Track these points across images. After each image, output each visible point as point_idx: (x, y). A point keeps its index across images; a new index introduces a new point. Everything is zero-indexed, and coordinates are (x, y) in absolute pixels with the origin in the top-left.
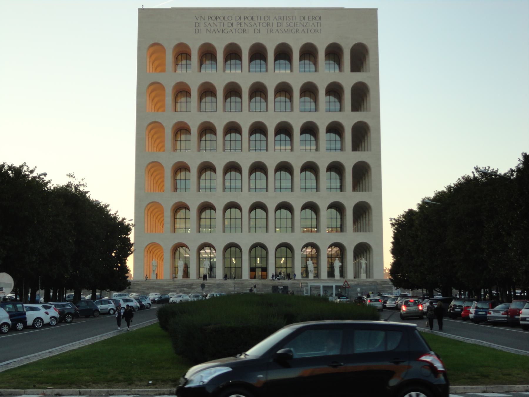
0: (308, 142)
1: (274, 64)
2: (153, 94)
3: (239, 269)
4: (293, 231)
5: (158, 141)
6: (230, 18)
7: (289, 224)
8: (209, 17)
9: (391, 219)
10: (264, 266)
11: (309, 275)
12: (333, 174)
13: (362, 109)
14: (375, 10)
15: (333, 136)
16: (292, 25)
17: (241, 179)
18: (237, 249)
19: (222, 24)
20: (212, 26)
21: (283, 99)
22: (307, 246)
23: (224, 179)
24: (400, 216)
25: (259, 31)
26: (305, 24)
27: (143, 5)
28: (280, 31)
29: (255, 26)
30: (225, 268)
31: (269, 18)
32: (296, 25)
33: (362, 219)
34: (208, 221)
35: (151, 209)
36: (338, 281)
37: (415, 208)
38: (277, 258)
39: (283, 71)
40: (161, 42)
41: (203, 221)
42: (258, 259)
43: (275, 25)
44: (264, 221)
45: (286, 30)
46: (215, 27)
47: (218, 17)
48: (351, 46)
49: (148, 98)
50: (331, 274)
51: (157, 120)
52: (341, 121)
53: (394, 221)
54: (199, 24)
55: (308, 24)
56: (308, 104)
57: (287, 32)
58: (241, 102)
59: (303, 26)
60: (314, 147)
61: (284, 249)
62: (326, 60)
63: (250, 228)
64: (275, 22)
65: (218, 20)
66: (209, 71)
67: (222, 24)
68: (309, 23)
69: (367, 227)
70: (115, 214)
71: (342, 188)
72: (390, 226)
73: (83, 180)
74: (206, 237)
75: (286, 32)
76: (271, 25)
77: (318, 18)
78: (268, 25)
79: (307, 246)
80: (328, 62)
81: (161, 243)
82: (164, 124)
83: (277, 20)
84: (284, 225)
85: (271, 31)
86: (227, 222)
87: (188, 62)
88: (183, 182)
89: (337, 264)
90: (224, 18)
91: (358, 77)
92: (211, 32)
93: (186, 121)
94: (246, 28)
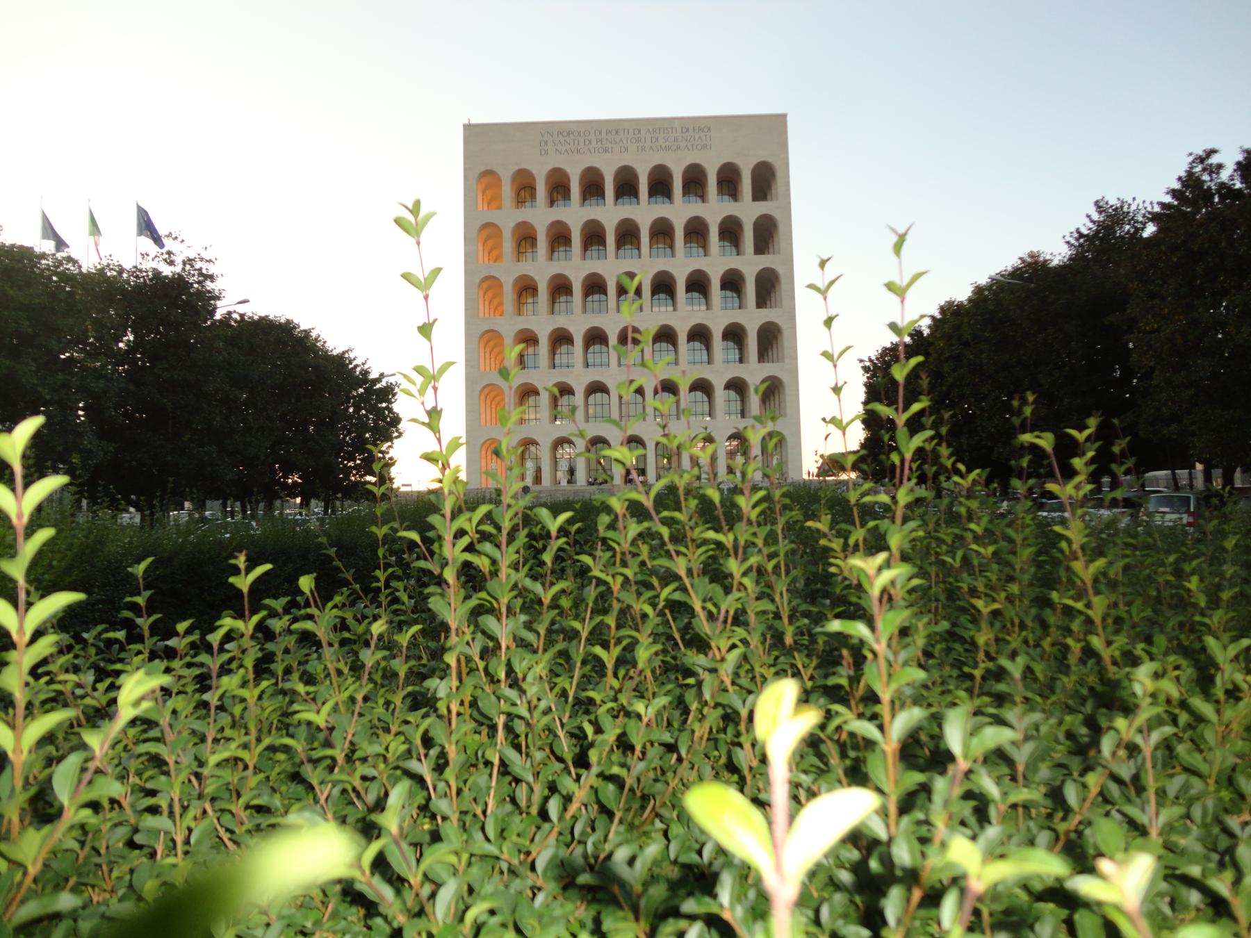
0: (696, 301)
6: (587, 133)
10: (641, 466)
12: (731, 344)
13: (771, 250)
15: (729, 293)
25: (627, 149)
31: (639, 131)
35: (492, 395)
43: (648, 141)
46: (568, 147)
48: (751, 166)
49: (481, 248)
52: (740, 268)
53: (868, 364)
54: (546, 143)
60: (704, 307)
64: (648, 136)
70: (363, 364)
71: (741, 361)
74: (563, 427)
77: (706, 130)
78: (639, 140)
82: (502, 280)
85: (643, 149)
86: (591, 411)
91: (762, 208)
93: (531, 274)
94: (609, 145)
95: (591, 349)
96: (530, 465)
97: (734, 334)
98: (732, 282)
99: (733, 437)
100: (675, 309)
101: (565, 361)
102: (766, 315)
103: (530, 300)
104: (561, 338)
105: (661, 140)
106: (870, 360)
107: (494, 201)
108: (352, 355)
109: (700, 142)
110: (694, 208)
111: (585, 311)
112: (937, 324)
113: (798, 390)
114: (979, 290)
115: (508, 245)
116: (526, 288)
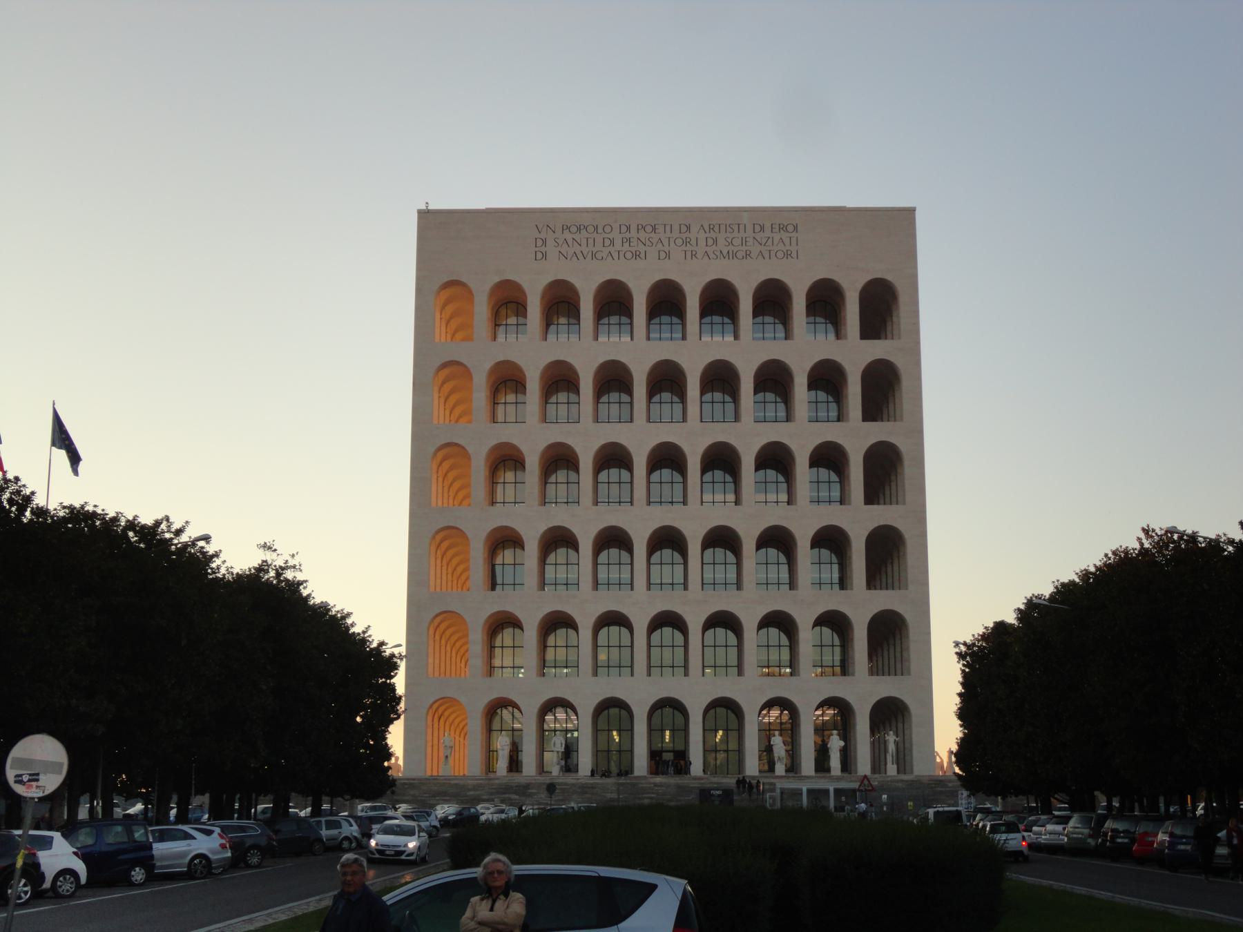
1: (701, 324)
2: (447, 387)
3: (627, 752)
4: (740, 672)
5: (457, 485)
6: (608, 229)
7: (733, 660)
8: (565, 227)
9: (957, 644)
10: (680, 747)
11: (776, 766)
12: (825, 553)
13: (885, 416)
14: (912, 211)
15: (824, 473)
16: (737, 242)
17: (632, 564)
18: (624, 712)
19: (591, 241)
20: (571, 246)
21: (718, 396)
22: (769, 704)
23: (595, 564)
24: (976, 636)
25: (668, 255)
26: (764, 241)
27: (427, 203)
28: (712, 256)
29: (660, 245)
30: (596, 752)
31: (688, 228)
32: (746, 241)
33: (885, 648)
34: (561, 653)
35: (443, 627)
36: (838, 779)
37: (1011, 619)
38: (708, 730)
39: (717, 338)
40: (464, 280)
41: (550, 652)
42: (668, 733)
43: (702, 243)
44: (680, 652)
45: (725, 253)
46: (577, 249)
47: (582, 227)
48: (860, 286)
49: (436, 396)
51: (455, 441)
53: (963, 648)
54: (544, 242)
55: (770, 240)
56: (771, 407)
57: (727, 257)
58: (631, 403)
59: (761, 244)
60: (784, 497)
61: (721, 711)
62: (808, 315)
63: (649, 667)
64: (702, 236)
65: (584, 232)
66: (563, 337)
67: (591, 241)
68: (773, 238)
69: (899, 666)
72: (955, 658)
75: (725, 258)
76: (693, 242)
77: (790, 228)
79: (769, 704)
80: (811, 319)
81: (462, 699)
82: (470, 449)
83: (705, 232)
84: (721, 662)
85: (694, 255)
86: (602, 656)
87: (521, 320)
88: (509, 569)
89: (835, 743)
90: (596, 228)
91: (877, 350)
92: (569, 258)
93: (515, 442)
94: (642, 248)
95: (603, 557)
100: (737, 502)
101: (562, 575)
102: (881, 515)
104: (559, 539)
105: (721, 241)
107: (461, 328)
109: (781, 246)
113: (929, 633)
115: (480, 395)
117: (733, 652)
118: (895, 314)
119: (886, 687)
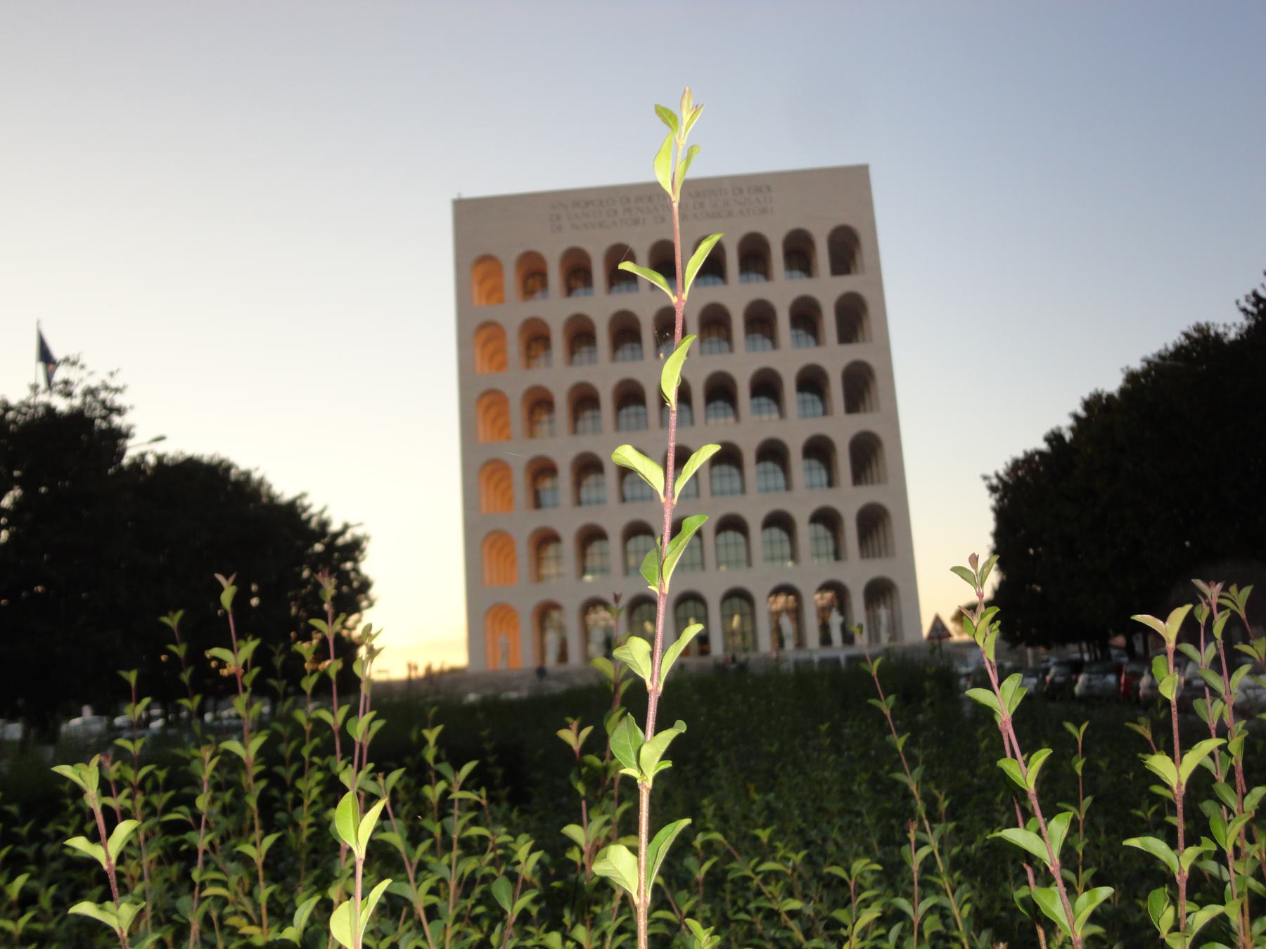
12: (815, 463)
13: (860, 336)
15: (808, 396)
21: (714, 339)
22: (777, 591)
38: (726, 617)
50: (826, 640)
53: (995, 481)
60: (775, 416)
61: (736, 602)
71: (831, 483)
73: (112, 374)
79: (777, 591)
89: (835, 620)
91: (846, 284)
96: (552, 638)
97: (819, 450)
98: (812, 381)
99: (826, 587)
103: (545, 418)
106: (997, 476)
107: (495, 294)
108: (306, 502)
110: (756, 289)
111: (617, 427)
112: (1081, 425)
114: (1132, 377)
115: (514, 346)
116: (539, 403)
117: (742, 550)
118: (858, 256)
119: (875, 569)
